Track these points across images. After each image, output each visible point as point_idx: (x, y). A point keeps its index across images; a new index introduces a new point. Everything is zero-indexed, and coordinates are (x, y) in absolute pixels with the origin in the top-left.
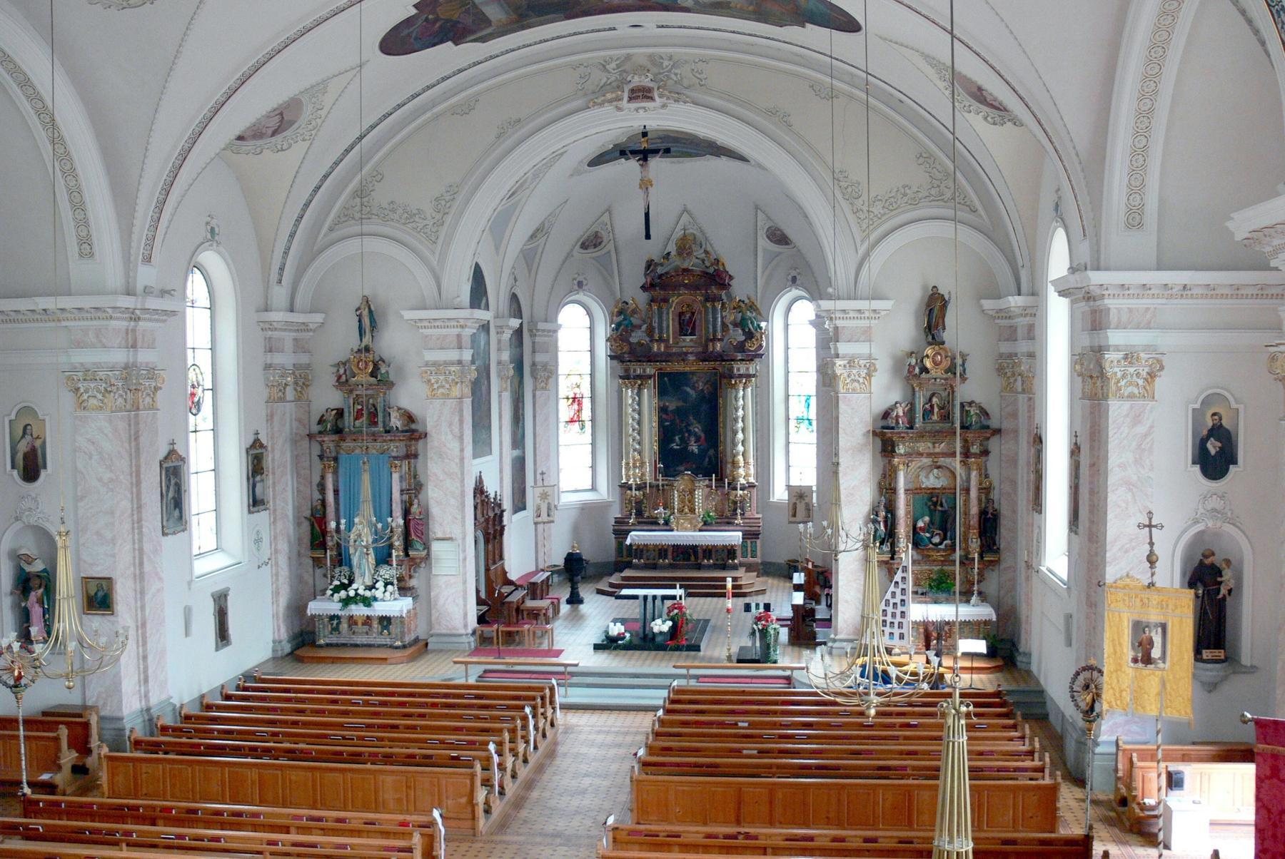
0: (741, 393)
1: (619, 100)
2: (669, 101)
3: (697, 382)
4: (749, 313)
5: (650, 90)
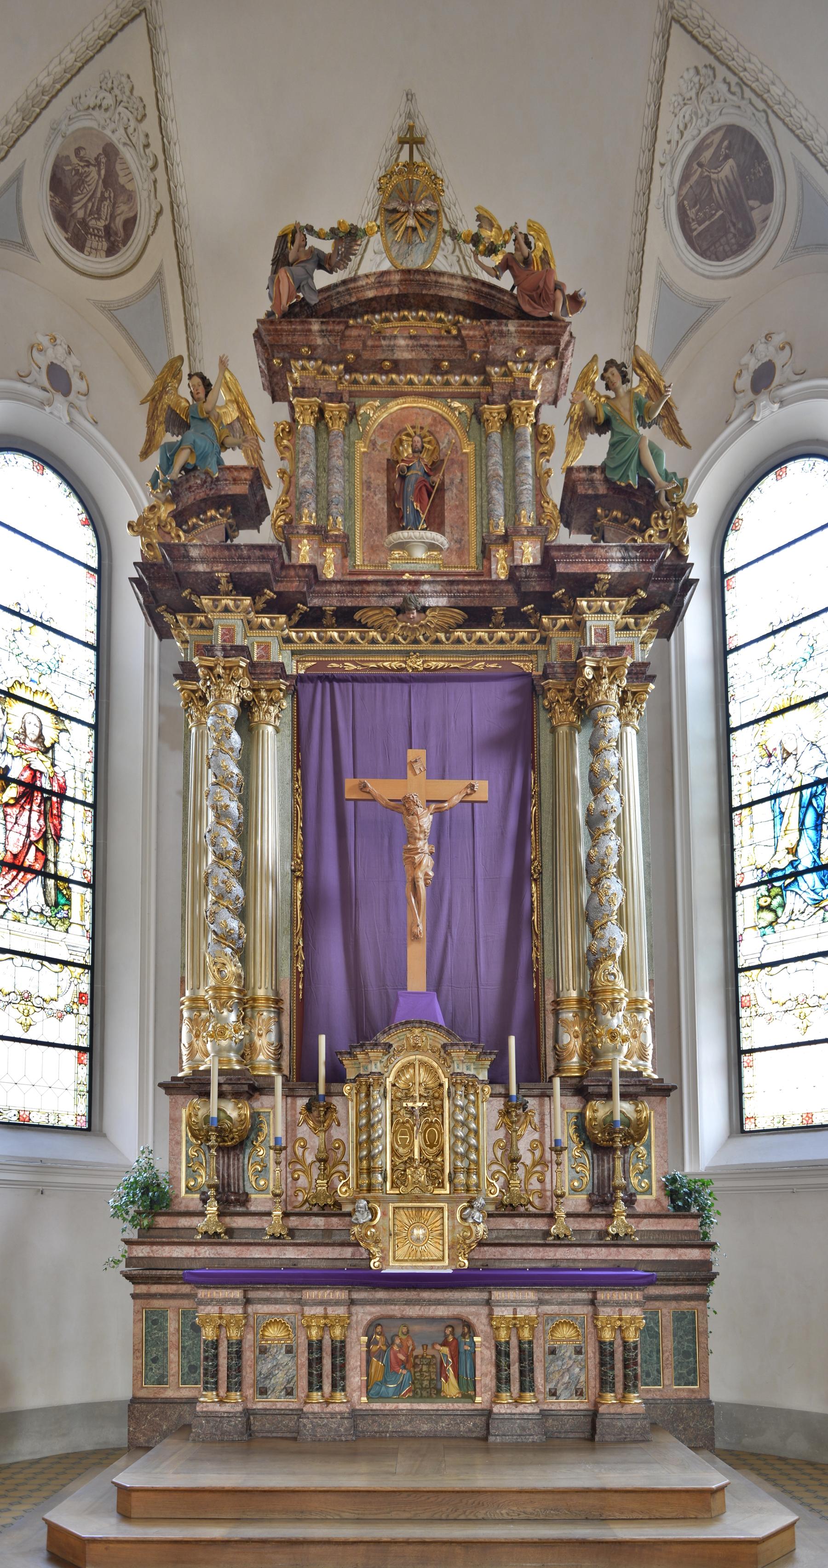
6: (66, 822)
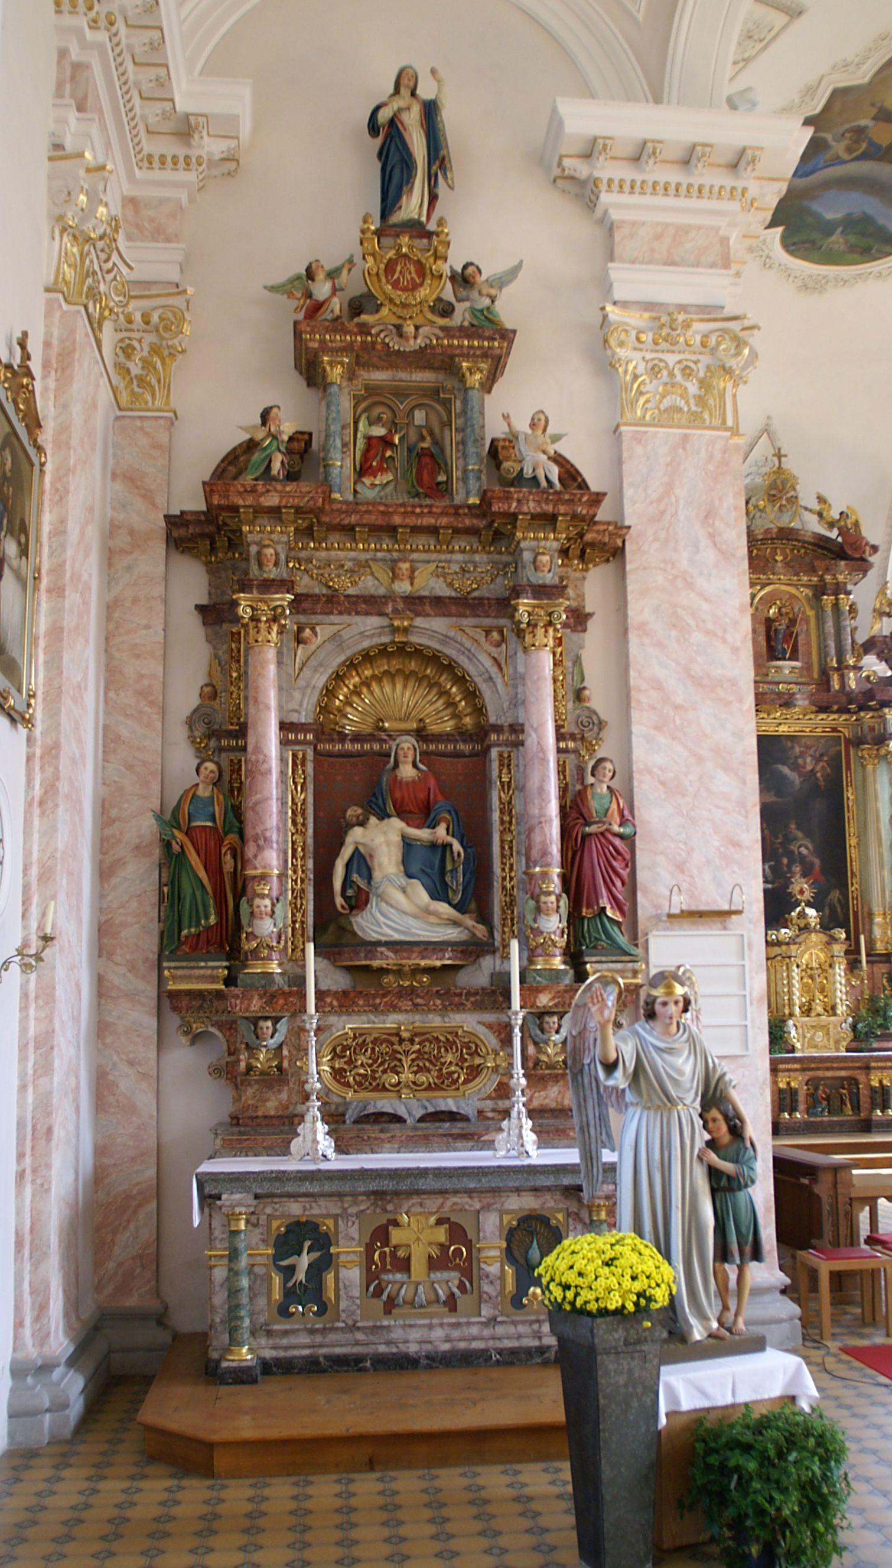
3: (802, 754)
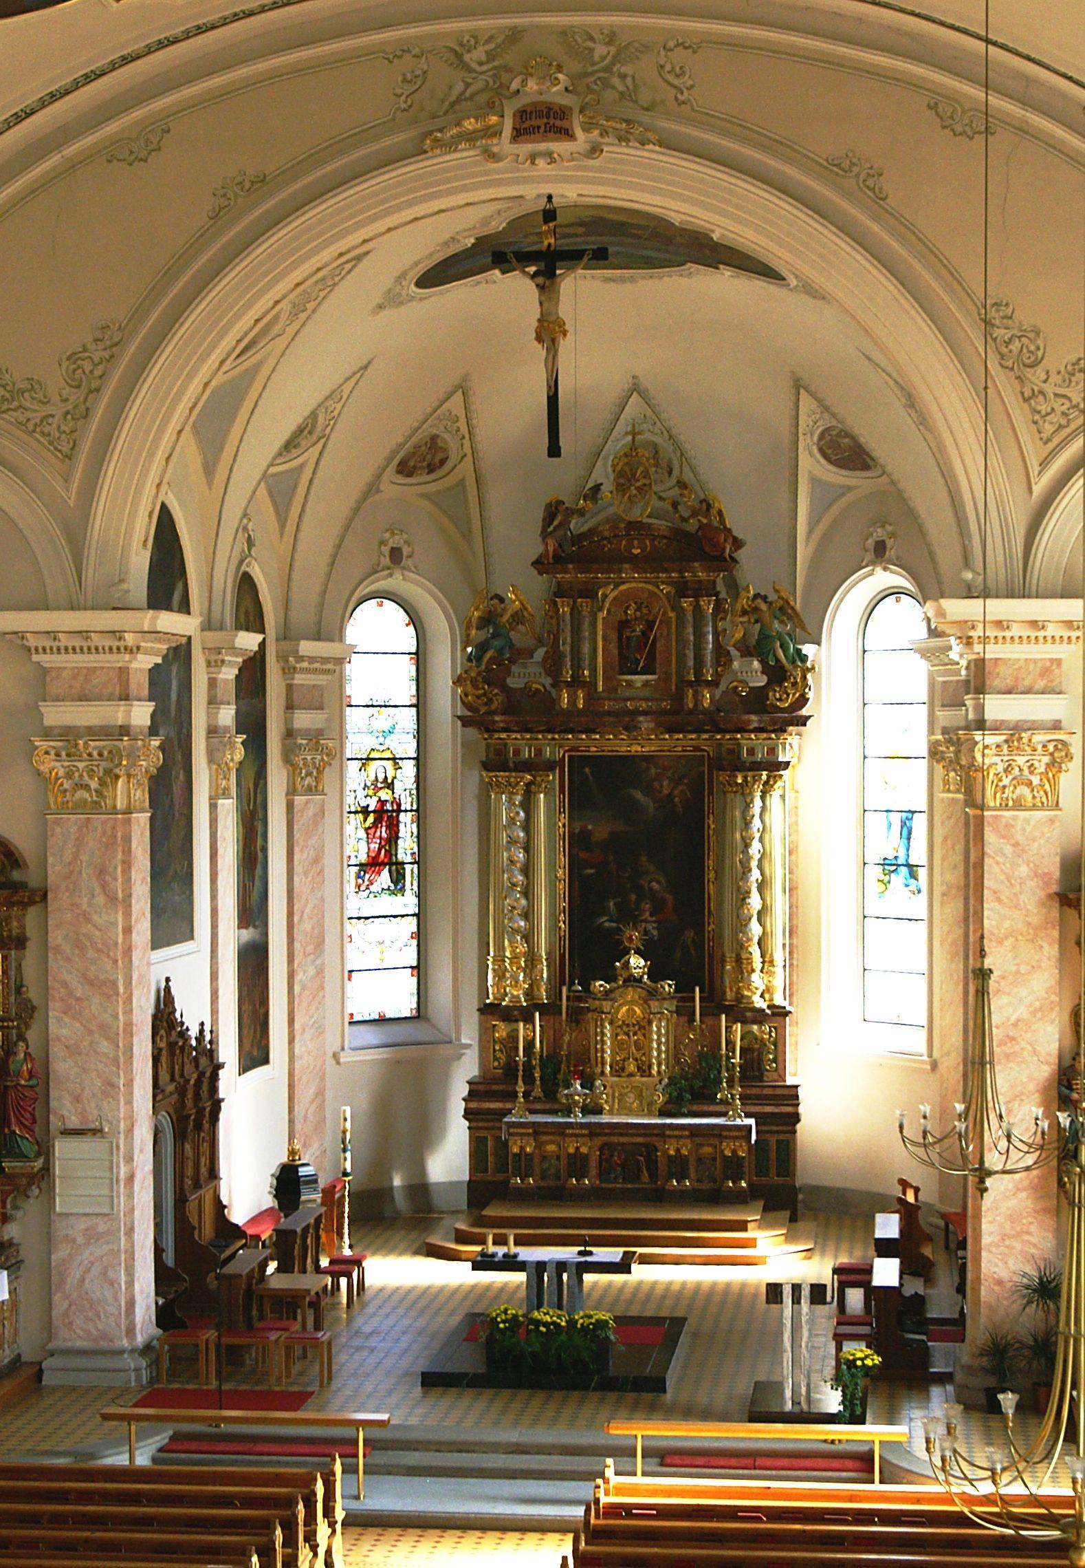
0: (758, 802)
1: (494, 135)
2: (606, 140)
4: (776, 625)
5: (563, 113)
6: (402, 826)
